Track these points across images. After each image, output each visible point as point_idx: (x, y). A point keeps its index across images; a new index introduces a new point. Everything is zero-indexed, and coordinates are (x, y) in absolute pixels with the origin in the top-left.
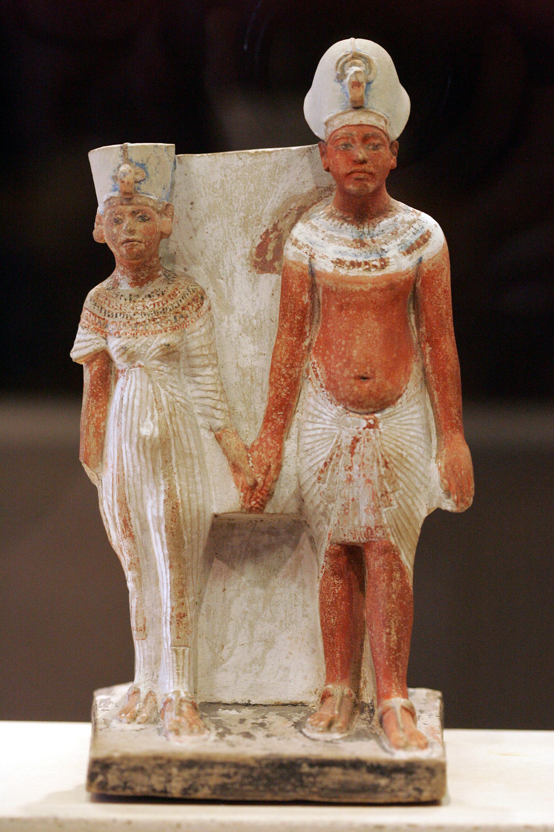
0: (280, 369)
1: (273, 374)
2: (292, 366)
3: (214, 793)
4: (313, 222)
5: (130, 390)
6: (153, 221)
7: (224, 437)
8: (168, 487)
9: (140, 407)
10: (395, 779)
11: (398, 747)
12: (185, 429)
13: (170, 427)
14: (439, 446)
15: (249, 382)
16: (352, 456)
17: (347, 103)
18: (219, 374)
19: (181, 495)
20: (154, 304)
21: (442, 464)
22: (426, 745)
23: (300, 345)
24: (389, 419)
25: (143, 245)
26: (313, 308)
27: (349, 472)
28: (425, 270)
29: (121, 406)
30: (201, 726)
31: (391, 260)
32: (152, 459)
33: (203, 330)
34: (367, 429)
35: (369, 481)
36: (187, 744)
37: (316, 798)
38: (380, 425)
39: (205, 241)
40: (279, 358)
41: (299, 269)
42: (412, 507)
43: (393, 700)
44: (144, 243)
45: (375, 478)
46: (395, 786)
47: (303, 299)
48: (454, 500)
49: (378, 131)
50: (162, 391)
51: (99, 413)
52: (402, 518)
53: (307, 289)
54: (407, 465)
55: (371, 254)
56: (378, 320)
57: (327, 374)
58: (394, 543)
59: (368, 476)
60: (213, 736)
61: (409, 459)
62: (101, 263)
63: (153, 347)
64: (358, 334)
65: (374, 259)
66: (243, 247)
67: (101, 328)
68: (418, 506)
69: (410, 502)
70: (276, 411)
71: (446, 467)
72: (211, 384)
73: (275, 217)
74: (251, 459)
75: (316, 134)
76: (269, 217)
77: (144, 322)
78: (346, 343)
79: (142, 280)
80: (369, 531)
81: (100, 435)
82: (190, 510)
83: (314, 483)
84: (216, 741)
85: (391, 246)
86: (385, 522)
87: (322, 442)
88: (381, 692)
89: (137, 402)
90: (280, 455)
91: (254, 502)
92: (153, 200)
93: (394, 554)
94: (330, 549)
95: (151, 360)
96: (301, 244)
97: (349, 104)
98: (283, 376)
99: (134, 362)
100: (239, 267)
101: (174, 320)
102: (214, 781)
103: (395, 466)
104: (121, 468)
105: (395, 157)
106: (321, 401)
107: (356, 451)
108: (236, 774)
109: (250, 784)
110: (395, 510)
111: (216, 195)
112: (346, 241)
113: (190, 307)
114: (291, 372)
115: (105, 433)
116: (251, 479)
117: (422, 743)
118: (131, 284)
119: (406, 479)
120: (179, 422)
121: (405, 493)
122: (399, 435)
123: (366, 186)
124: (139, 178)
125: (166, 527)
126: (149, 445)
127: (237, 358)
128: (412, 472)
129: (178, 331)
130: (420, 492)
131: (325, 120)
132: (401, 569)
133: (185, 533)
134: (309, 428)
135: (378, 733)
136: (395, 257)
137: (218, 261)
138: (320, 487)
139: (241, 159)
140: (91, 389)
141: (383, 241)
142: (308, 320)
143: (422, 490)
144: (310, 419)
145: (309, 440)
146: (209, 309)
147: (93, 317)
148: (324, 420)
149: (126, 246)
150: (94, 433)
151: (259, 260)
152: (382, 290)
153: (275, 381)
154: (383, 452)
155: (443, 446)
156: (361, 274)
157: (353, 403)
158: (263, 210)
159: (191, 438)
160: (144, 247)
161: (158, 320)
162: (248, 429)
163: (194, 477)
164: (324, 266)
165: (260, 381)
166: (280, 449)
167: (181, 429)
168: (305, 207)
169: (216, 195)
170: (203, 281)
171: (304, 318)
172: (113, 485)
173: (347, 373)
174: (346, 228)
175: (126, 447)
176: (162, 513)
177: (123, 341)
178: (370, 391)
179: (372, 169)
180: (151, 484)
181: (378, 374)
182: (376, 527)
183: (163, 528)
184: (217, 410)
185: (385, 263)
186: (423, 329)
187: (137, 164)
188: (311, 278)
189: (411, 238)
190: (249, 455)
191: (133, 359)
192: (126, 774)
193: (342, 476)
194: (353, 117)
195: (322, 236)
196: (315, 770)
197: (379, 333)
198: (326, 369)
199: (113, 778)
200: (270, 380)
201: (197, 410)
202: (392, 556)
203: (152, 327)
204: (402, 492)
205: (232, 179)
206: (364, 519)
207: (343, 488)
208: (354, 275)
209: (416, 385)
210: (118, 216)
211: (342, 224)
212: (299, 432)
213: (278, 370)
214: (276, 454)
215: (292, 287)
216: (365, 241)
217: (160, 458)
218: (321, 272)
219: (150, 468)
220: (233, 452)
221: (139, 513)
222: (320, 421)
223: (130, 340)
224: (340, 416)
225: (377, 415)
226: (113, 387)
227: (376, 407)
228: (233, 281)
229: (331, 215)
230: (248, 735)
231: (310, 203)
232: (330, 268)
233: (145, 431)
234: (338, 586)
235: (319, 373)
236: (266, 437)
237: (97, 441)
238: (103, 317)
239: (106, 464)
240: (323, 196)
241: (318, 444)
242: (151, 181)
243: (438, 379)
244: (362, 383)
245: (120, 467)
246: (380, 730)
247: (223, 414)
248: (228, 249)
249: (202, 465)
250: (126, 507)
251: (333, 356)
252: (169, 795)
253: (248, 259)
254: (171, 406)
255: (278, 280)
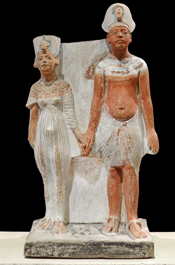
0: (94, 108)
1: (92, 110)
2: (98, 107)
3: (70, 256)
4: (105, 61)
5: (44, 115)
6: (53, 59)
7: (75, 131)
8: (56, 148)
9: (47, 121)
10: (135, 249)
11: (136, 237)
12: (62, 128)
13: (57, 127)
14: (147, 133)
15: (84, 114)
16: (118, 136)
17: (116, 19)
18: (74, 111)
19: (61, 150)
20: (53, 87)
21: (148, 138)
22: (146, 237)
23: (100, 100)
24: (130, 123)
25: (49, 67)
26: (105, 88)
27: (117, 141)
28: (141, 75)
29: (41, 122)
30: (66, 230)
31: (130, 71)
32: (51, 138)
33: (69, 96)
34: (123, 126)
35: (124, 144)
36: (61, 237)
37: (107, 257)
38: (128, 125)
39: (70, 70)
40: (93, 105)
41: (100, 76)
42: (139, 153)
43: (133, 220)
44: (50, 66)
45: (126, 143)
46: (135, 252)
47: (102, 85)
48: (152, 151)
49: (126, 28)
50: (55, 116)
51: (35, 124)
52: (135, 157)
53: (103, 82)
54: (137, 138)
55: (124, 69)
56: (126, 90)
57: (110, 108)
58: (132, 165)
59: (124, 142)
60: (70, 234)
61: (137, 136)
62: (35, 75)
63: (52, 101)
64: (120, 95)
65: (125, 70)
66: (82, 71)
67: (36, 96)
68: (141, 153)
69: (138, 151)
70: (93, 122)
71: (149, 139)
72: (71, 114)
73: (92, 62)
74: (84, 138)
75: (106, 31)
76: (91, 62)
77: (49, 93)
78: (116, 98)
79: (49, 80)
80: (124, 161)
81: (35, 132)
82: (64, 156)
83: (105, 146)
84: (71, 236)
85: (130, 67)
86: (130, 158)
87: (108, 131)
88: (129, 218)
89: (46, 119)
90: (94, 136)
91: (85, 152)
92: (53, 53)
93: (133, 169)
94: (111, 169)
95: (51, 105)
96: (101, 68)
97: (117, 20)
98: (95, 110)
99: (46, 106)
100: (81, 78)
101: (59, 93)
102: (70, 251)
103: (133, 138)
104: (41, 142)
105: (131, 39)
106: (107, 118)
107: (119, 134)
108: (78, 248)
109: (83, 252)
110: (133, 154)
111: (74, 55)
112: (116, 65)
113: (65, 88)
114: (97, 109)
115: (36, 131)
116: (84, 144)
117: (145, 236)
118: (45, 81)
119: (136, 143)
120: (61, 126)
121: (136, 148)
122: (134, 128)
123: (122, 45)
124: (48, 45)
125: (55, 161)
126: (50, 133)
127: (80, 107)
128: (138, 141)
129: (61, 96)
130: (141, 148)
131: (109, 26)
132: (135, 175)
133: (62, 163)
134: (103, 127)
135: (128, 233)
136: (131, 70)
137: (74, 76)
138: (107, 147)
139: (82, 44)
140: (32, 116)
141: (128, 65)
142: (103, 92)
143: (142, 147)
144: (104, 124)
145: (104, 131)
146: (71, 90)
147: (33, 93)
148: (109, 124)
149: (43, 67)
150: (33, 131)
151: (87, 75)
152: (127, 80)
153: (92, 112)
154: (129, 134)
155: (148, 133)
156: (121, 75)
157: (118, 118)
158: (88, 60)
159: (65, 132)
160: (49, 68)
161: (54, 92)
162: (83, 129)
163: (65, 144)
164: (108, 73)
165: (87, 114)
166: (94, 135)
167: (61, 128)
168: (102, 58)
169: (74, 55)
170: (69, 82)
171: (102, 91)
172: (38, 148)
173: (116, 107)
174: (116, 62)
175: (42, 135)
176: (54, 157)
177: (42, 99)
178: (124, 113)
179: (124, 40)
180: (51, 147)
181: (127, 107)
182: (126, 160)
183: (54, 162)
184: (73, 122)
185: (128, 72)
186: (141, 95)
187: (48, 41)
188: (104, 79)
189: (137, 65)
190: (84, 137)
191: (45, 105)
192: (38, 249)
193: (115, 143)
194: (118, 24)
195: (108, 64)
196: (106, 246)
197: (127, 95)
198: (109, 107)
199: (33, 250)
200: (91, 112)
201: (67, 123)
202: (132, 170)
203: (52, 94)
204: (135, 148)
205: (79, 50)
206: (123, 157)
207: (115, 147)
208: (118, 76)
209: (139, 112)
210: (41, 58)
211: (114, 60)
212: (100, 129)
213: (93, 109)
214: (93, 136)
215: (98, 81)
216: (122, 65)
217: (54, 138)
218: (107, 76)
219: (51, 141)
220: (78, 136)
221: (47, 157)
222: (107, 124)
223: (45, 99)
224: (114, 122)
225: (126, 121)
226: (39, 116)
227: (126, 119)
228: (79, 82)
229: (111, 58)
230: (83, 234)
231: (104, 57)
232: (110, 74)
233: (49, 129)
234: (113, 182)
235: (107, 109)
236: (89, 131)
237: (34, 134)
238: (36, 92)
239: (36, 141)
240: (108, 55)
241: (107, 132)
242: (52, 47)
243: (146, 111)
244: (121, 110)
245: (41, 142)
246: (129, 231)
247: (75, 124)
248: (77, 72)
249: (68, 141)
250: (42, 155)
251: (111, 103)
252: (54, 257)
253: (84, 75)
254: (58, 120)
255: (93, 81)
